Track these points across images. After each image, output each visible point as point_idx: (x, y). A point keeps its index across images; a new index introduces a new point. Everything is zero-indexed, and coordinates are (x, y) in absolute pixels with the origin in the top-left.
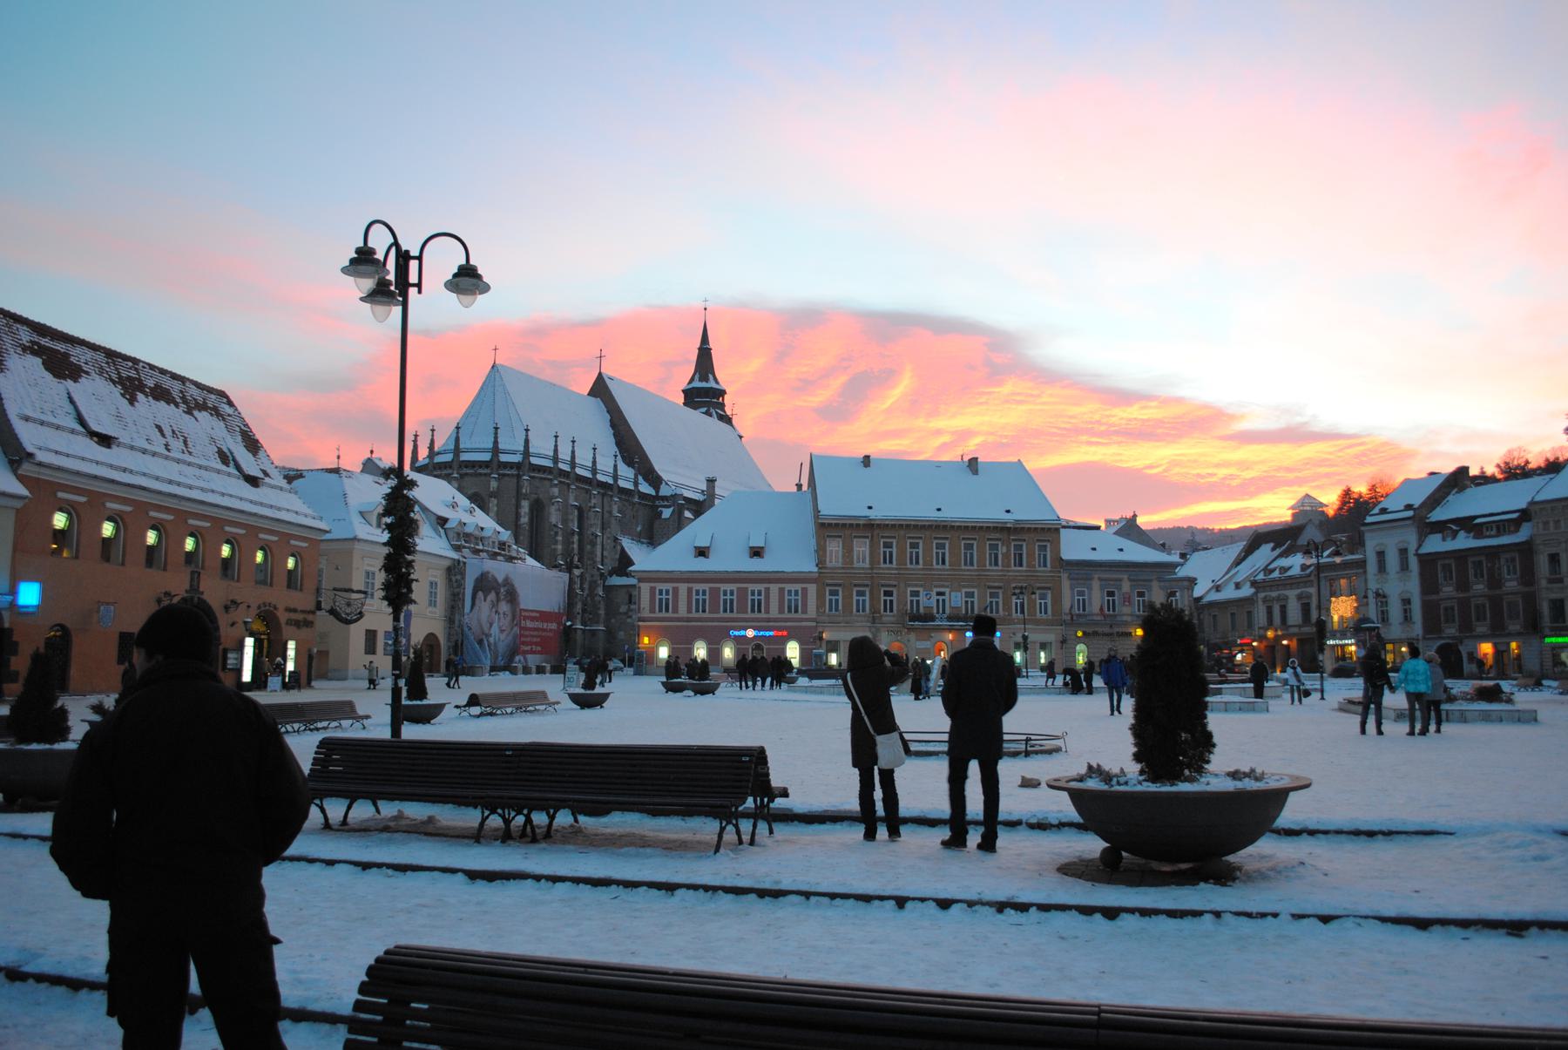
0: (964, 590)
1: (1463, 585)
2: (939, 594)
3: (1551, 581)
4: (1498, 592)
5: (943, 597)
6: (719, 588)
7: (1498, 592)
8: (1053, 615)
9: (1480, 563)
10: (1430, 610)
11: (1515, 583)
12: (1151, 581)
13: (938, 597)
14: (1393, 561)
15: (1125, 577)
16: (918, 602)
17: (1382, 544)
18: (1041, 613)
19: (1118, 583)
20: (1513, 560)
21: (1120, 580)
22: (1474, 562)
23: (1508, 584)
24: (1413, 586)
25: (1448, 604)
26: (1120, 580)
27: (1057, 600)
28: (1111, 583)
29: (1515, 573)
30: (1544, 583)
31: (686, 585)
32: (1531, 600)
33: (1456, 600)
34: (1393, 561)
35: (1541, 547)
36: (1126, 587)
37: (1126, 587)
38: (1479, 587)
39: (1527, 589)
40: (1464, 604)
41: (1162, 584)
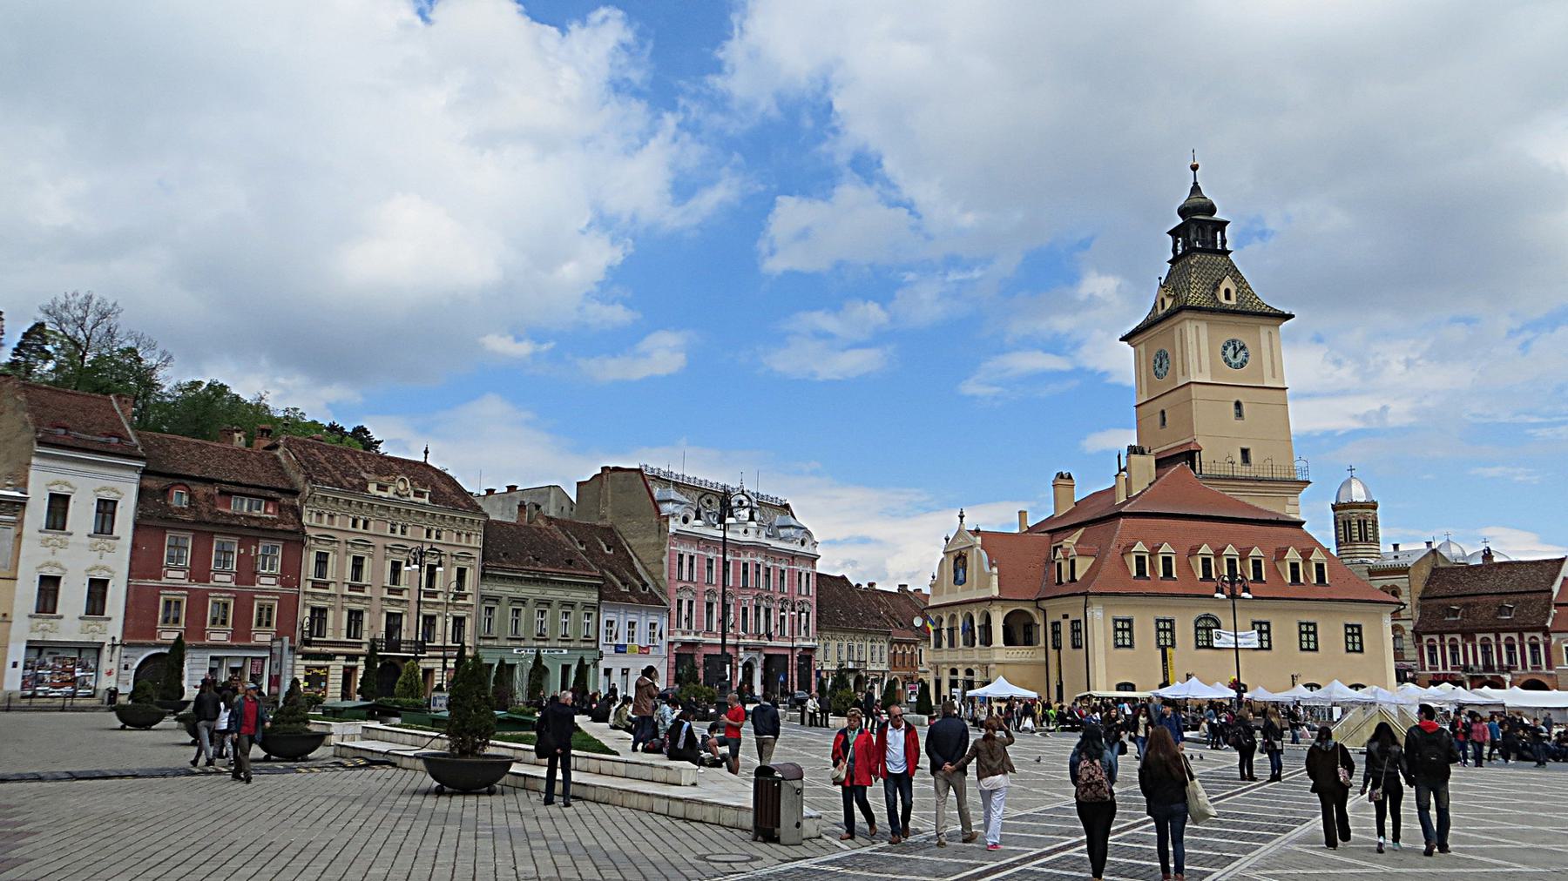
1: (200, 572)
3: (315, 584)
4: (248, 589)
7: (248, 589)
11: (273, 581)
14: (82, 515)
17: (66, 484)
22: (218, 542)
23: (263, 580)
24: (116, 562)
25: (173, 595)
32: (289, 605)
33: (186, 592)
34: (82, 515)
35: (313, 542)
38: (224, 579)
39: (288, 591)
40: (198, 600)
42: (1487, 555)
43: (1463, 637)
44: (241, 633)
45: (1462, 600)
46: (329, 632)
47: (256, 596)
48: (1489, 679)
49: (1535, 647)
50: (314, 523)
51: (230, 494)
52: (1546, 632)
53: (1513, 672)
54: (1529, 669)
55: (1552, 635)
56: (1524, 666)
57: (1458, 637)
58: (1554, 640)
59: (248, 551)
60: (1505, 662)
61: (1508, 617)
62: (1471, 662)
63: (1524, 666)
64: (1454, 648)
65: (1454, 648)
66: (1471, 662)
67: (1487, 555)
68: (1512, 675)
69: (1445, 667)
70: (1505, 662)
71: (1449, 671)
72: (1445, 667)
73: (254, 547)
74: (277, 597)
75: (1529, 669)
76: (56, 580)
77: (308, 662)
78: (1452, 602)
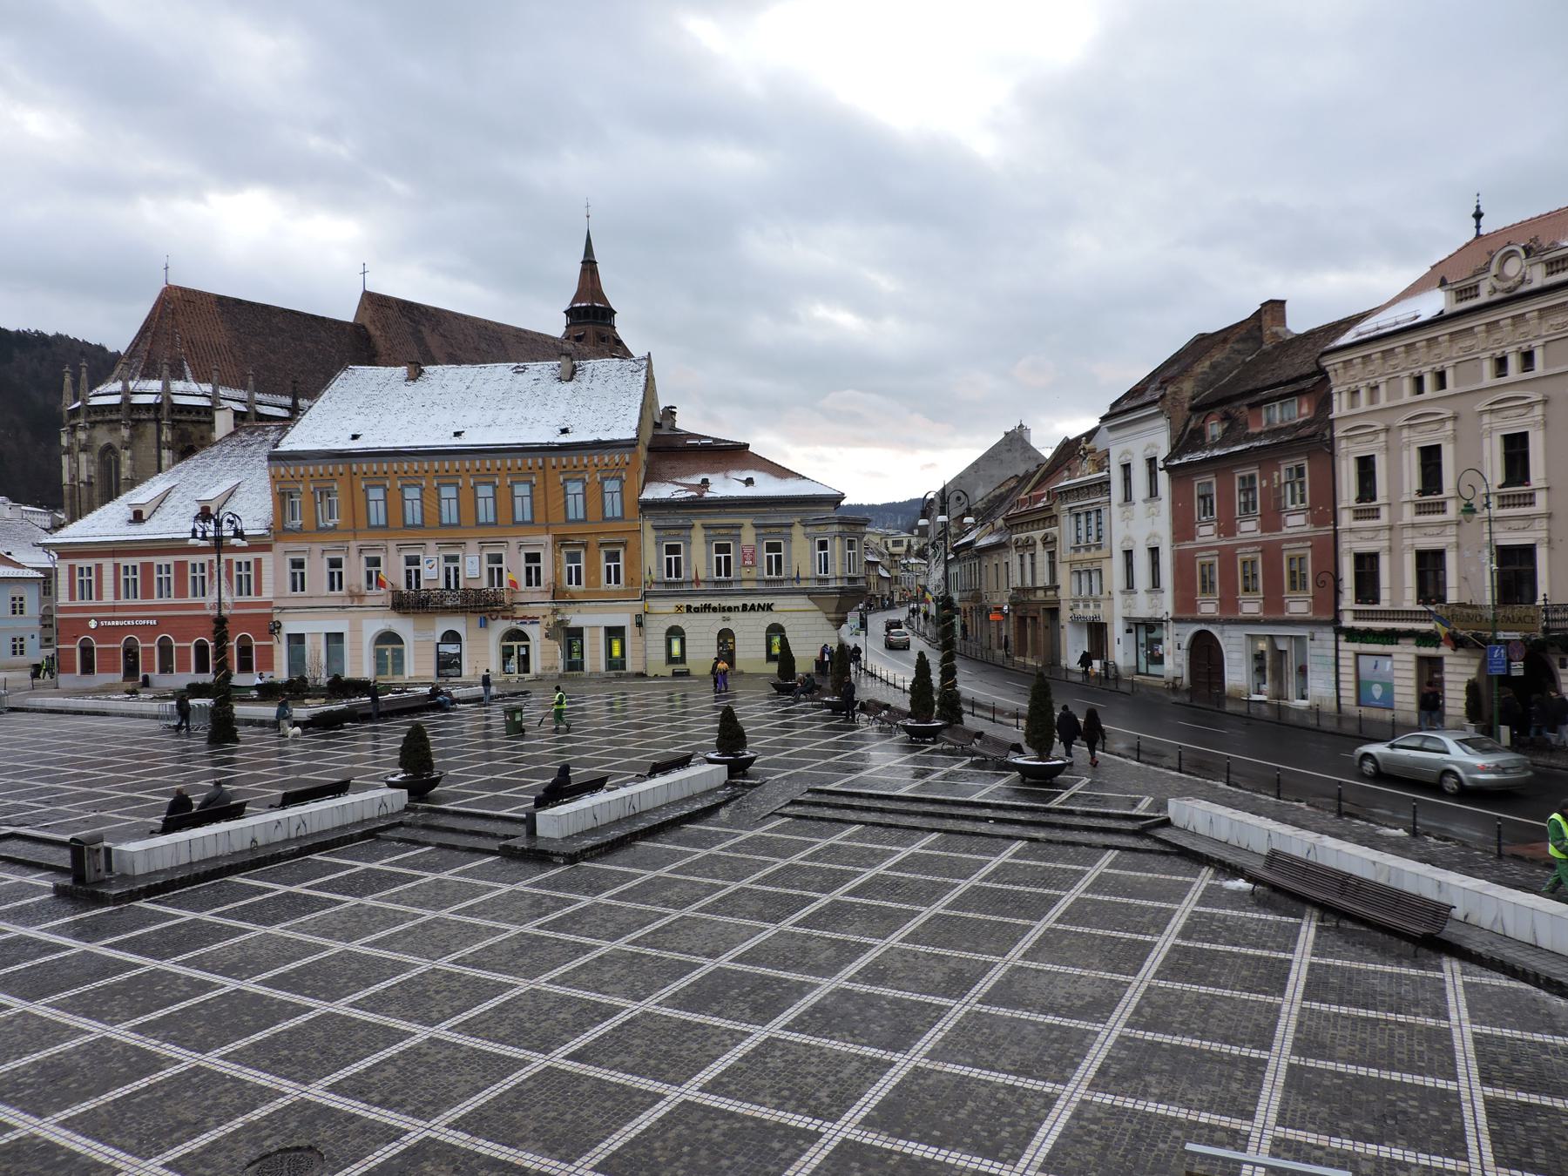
0: (486, 552)
2: (448, 559)
3: (1359, 514)
5: (456, 565)
6: (186, 562)
8: (626, 585)
9: (1252, 477)
10: (1183, 563)
12: (790, 526)
13: (448, 565)
15: (747, 522)
16: (418, 572)
18: (609, 581)
19: (734, 532)
20: (1300, 472)
21: (740, 527)
23: (1292, 521)
26: (740, 527)
27: (635, 561)
28: (723, 531)
29: (1303, 501)
30: (1346, 520)
31: (111, 559)
33: (1216, 552)
36: (748, 536)
37: (748, 536)
41: (808, 530)
44: (1274, 601)
46: (1384, 594)
47: (1285, 546)
50: (1345, 411)
51: (1258, 405)
59: (1271, 481)
73: (1276, 474)
74: (1309, 544)
76: (1157, 549)
77: (1356, 647)
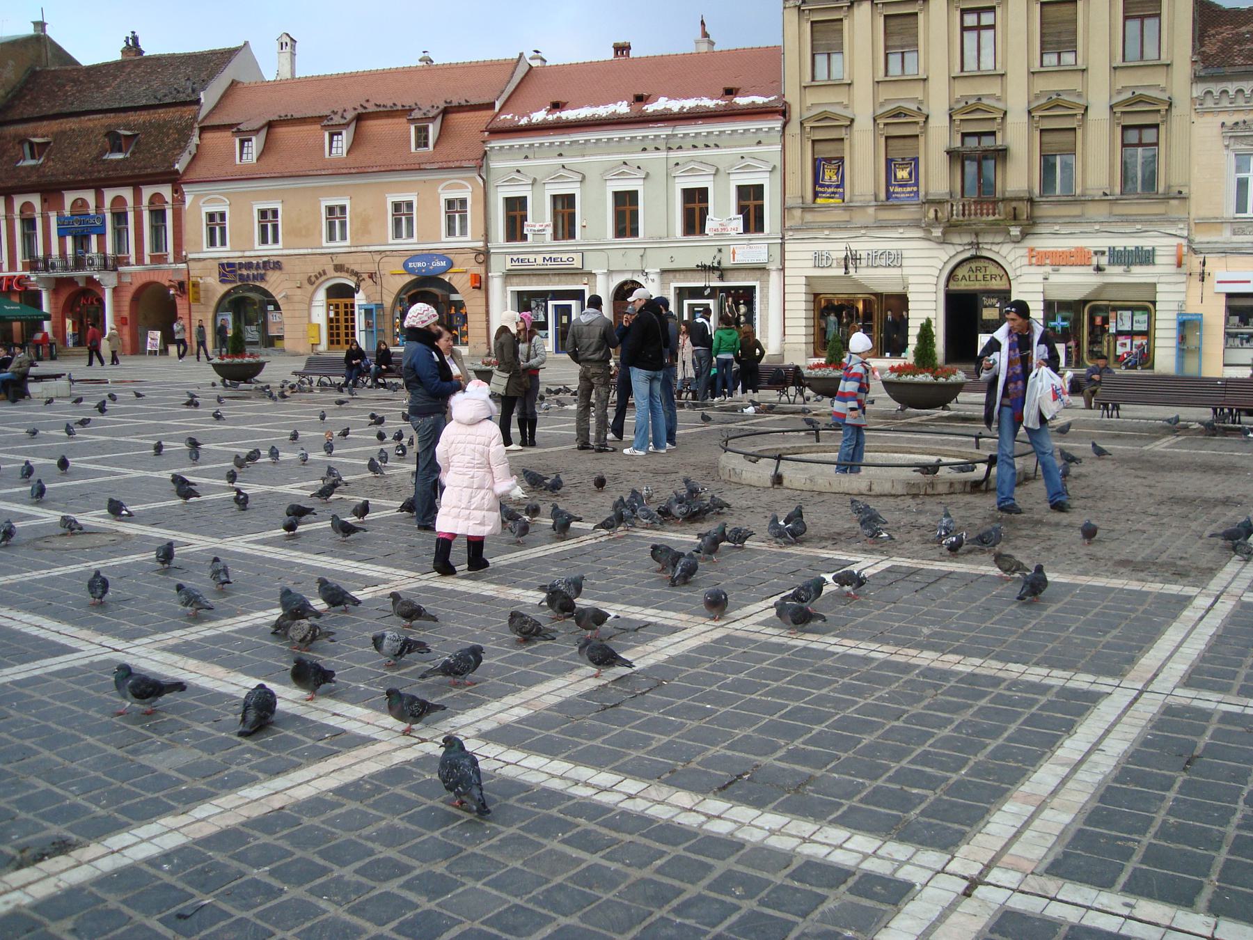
42: (133, 46)
43: (44, 201)
45: (55, 126)
48: (81, 284)
49: (158, 215)
52: (175, 180)
53: (120, 269)
54: (147, 260)
55: (185, 188)
56: (140, 260)
57: (36, 200)
58: (189, 199)
60: (109, 250)
61: (120, 156)
62: (55, 251)
63: (140, 260)
64: (29, 223)
65: (29, 223)
66: (55, 251)
67: (133, 46)
68: (120, 276)
69: (12, 265)
70: (109, 250)
71: (19, 272)
72: (12, 265)
75: (147, 260)
78: (30, 131)
